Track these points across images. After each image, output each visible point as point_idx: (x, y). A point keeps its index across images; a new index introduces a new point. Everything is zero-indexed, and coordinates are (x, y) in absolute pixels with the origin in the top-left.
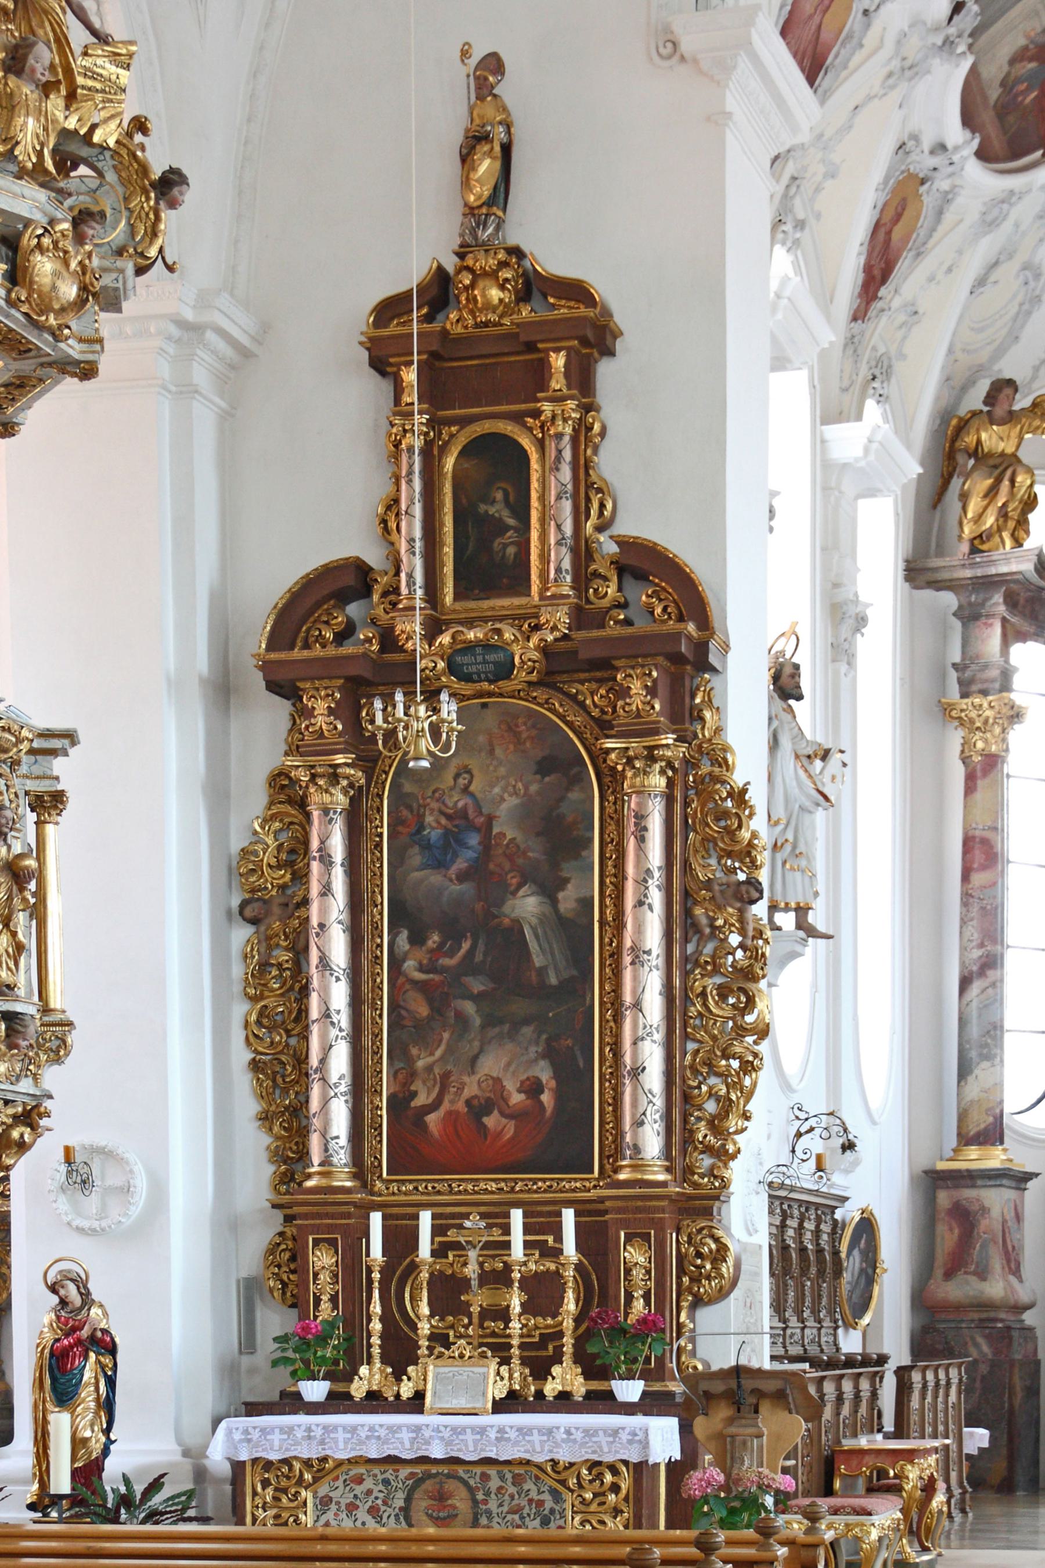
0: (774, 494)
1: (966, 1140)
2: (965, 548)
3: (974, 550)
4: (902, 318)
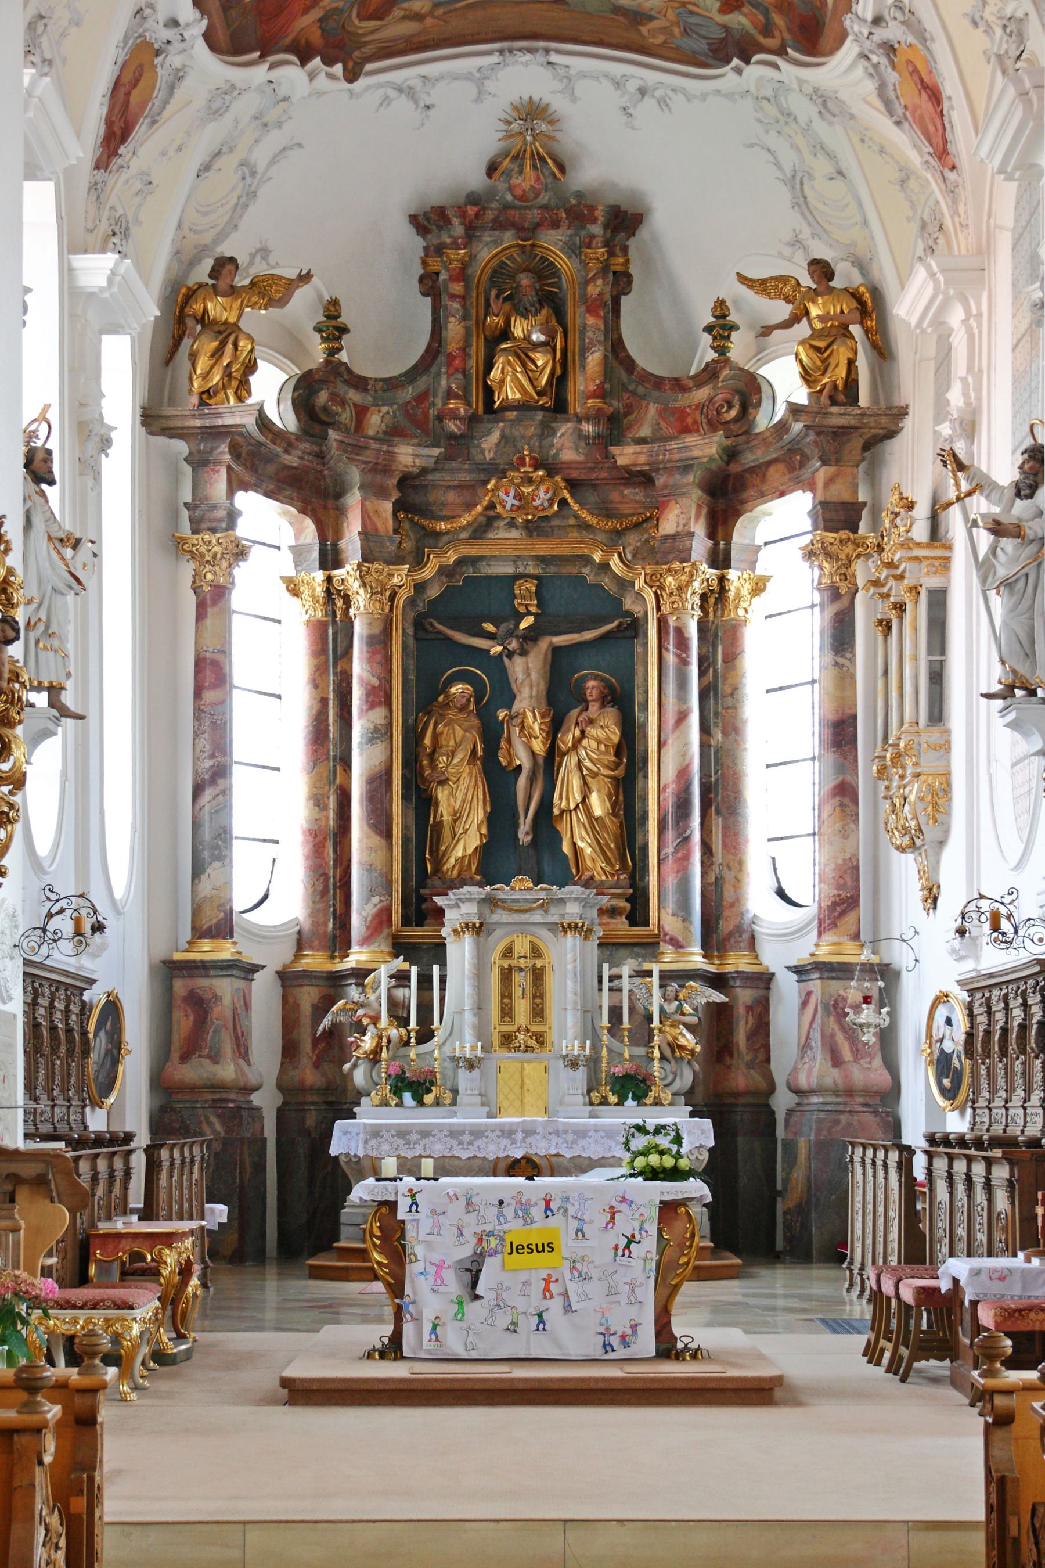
0: (27, 290)
1: (200, 933)
2: (195, 400)
3: (202, 403)
4: (138, 185)
